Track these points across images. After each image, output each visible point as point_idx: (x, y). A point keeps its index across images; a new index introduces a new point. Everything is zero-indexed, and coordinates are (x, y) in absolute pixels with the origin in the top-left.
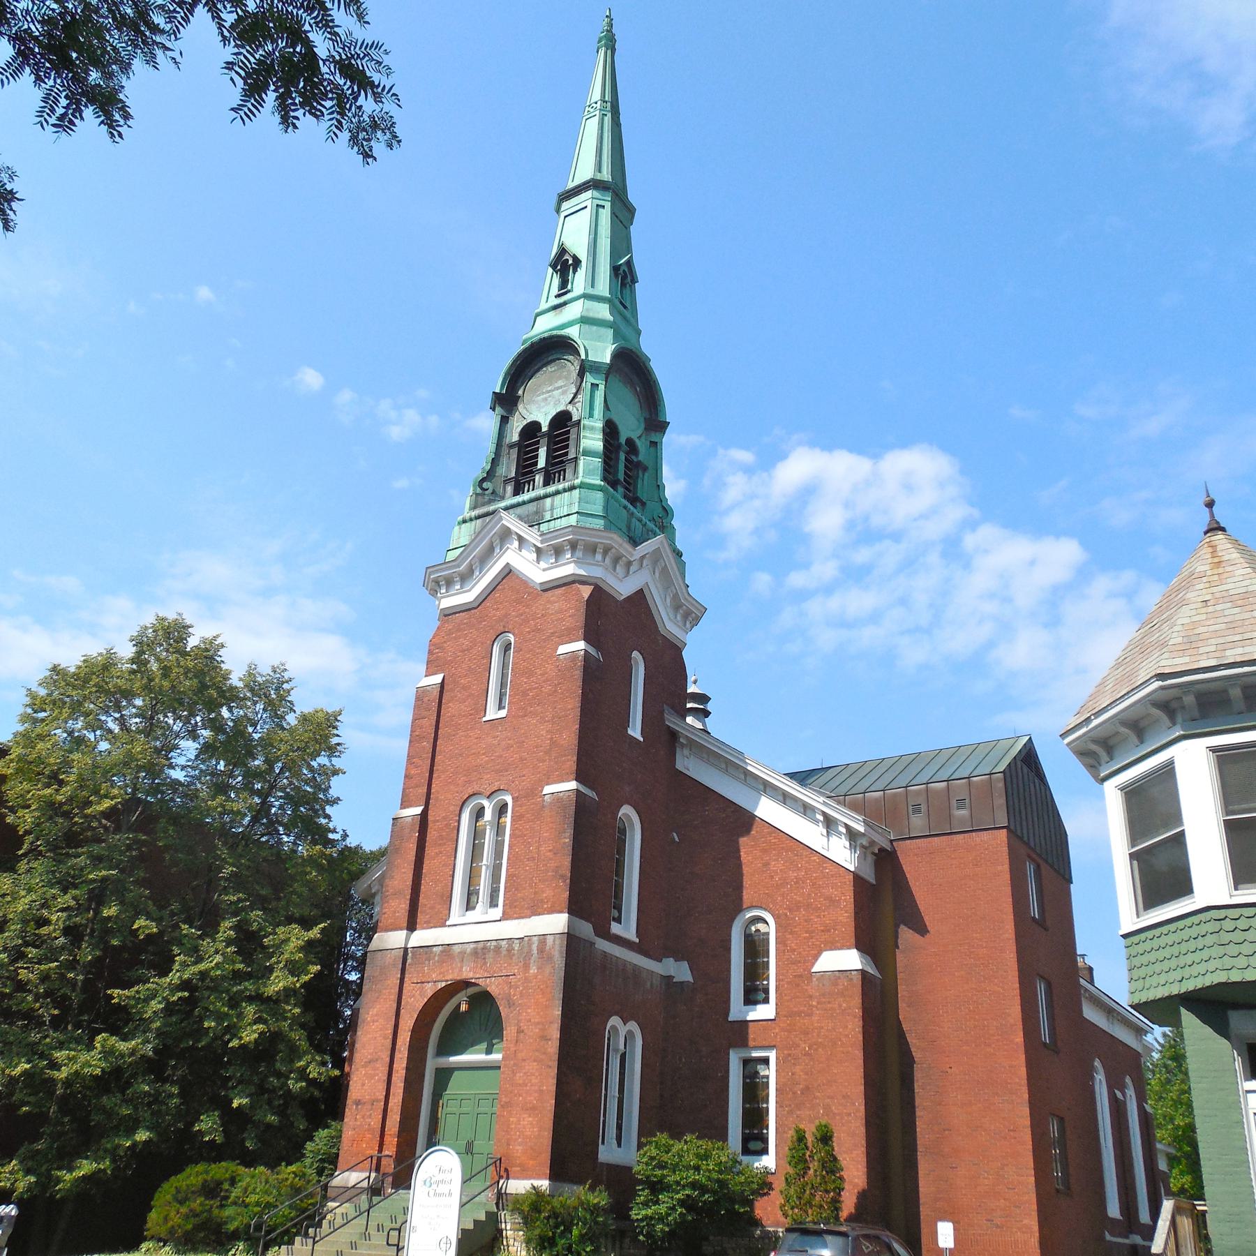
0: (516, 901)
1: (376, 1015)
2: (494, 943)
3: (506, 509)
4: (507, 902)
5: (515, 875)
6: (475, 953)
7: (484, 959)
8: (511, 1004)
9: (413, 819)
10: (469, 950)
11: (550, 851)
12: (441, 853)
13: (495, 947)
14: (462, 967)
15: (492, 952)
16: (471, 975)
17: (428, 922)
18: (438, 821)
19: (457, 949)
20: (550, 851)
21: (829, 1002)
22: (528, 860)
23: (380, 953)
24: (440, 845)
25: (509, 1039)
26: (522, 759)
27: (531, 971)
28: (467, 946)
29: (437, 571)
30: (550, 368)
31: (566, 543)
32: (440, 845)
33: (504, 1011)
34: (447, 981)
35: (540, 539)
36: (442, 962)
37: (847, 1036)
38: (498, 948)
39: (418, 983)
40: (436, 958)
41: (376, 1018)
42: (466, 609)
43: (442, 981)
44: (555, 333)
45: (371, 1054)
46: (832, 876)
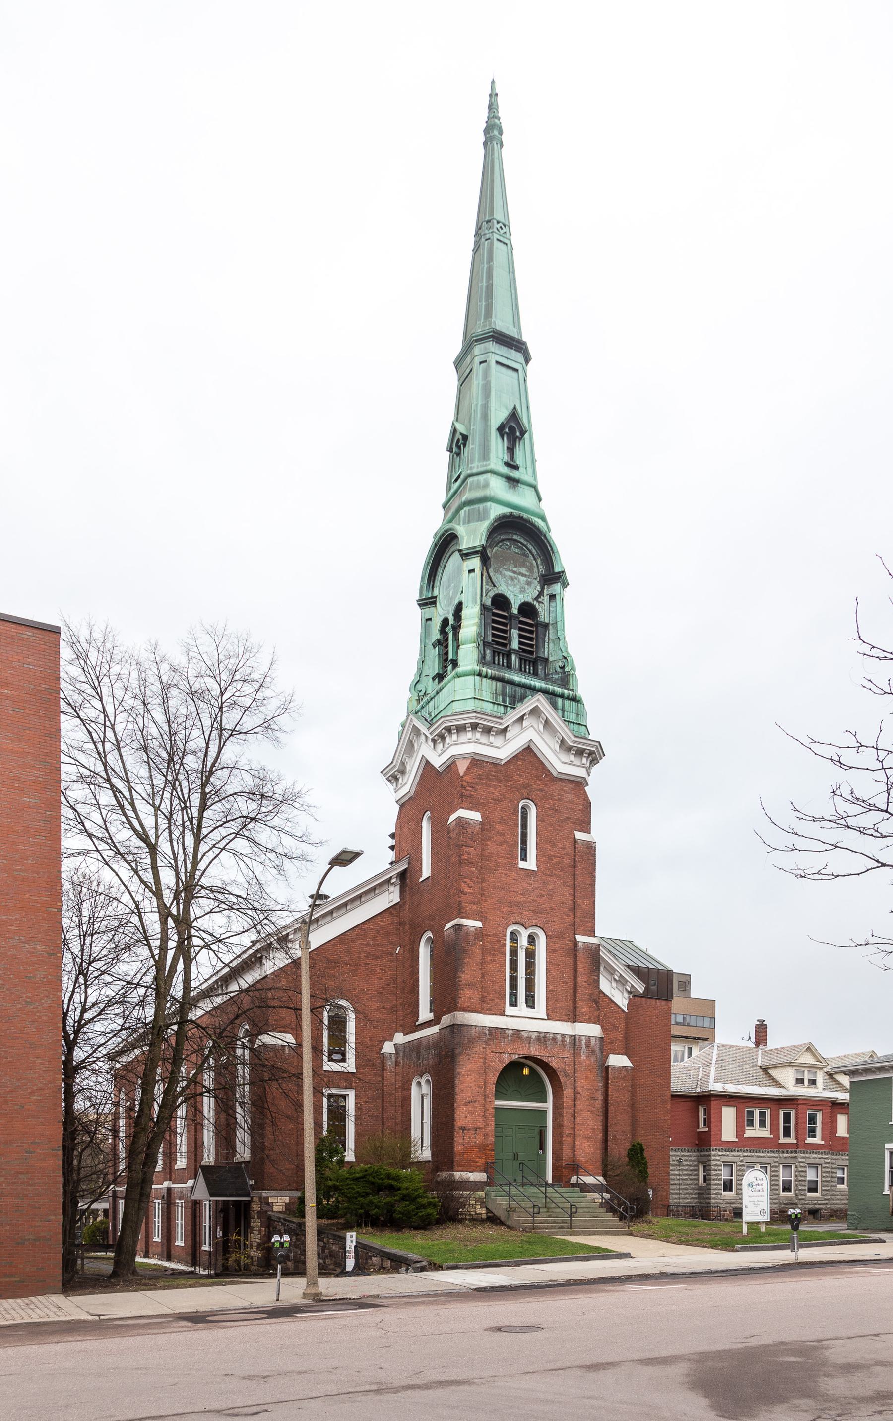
0: (556, 1009)
1: (469, 1071)
2: (552, 1035)
5: (554, 991)
6: (538, 1039)
7: (546, 1044)
10: (534, 1037)
14: (529, 1047)
16: (537, 1053)
19: (525, 1035)
28: (532, 1033)
34: (519, 1054)
45: (470, 1097)
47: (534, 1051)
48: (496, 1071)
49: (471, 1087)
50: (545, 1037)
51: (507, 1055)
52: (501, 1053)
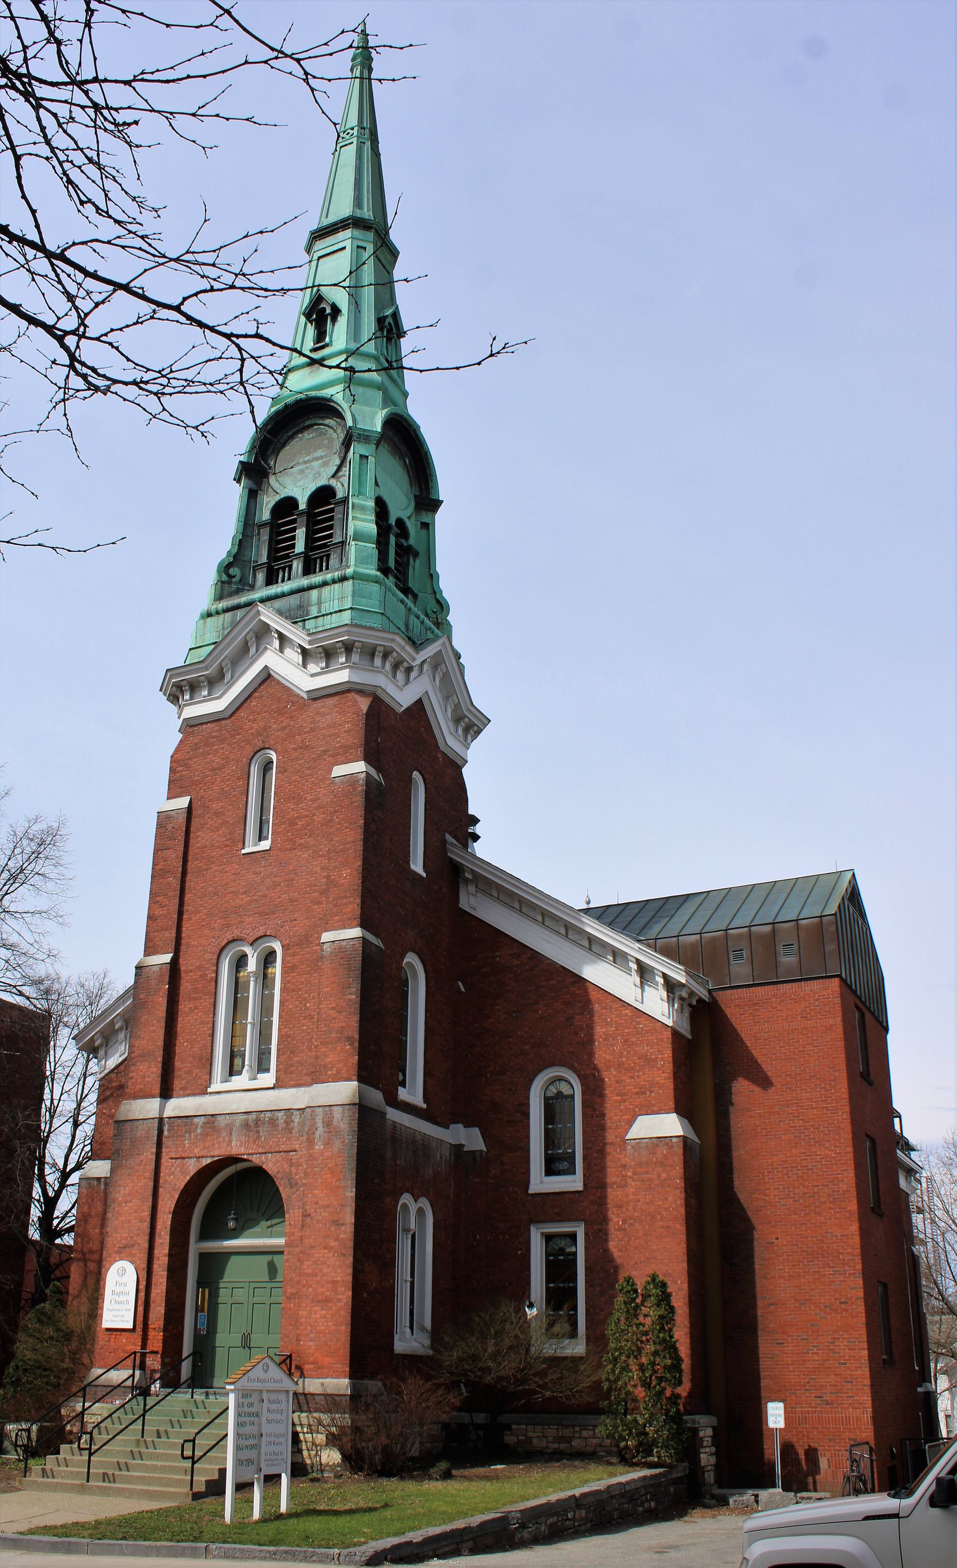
0: (292, 1065)
1: (129, 1195)
2: (268, 1114)
3: (263, 601)
4: (281, 1067)
5: (289, 1036)
7: (258, 1132)
8: (292, 1184)
9: (161, 969)
10: (238, 1123)
11: (333, 1008)
12: (196, 1008)
13: (271, 1119)
15: (266, 1125)
16: (243, 1150)
17: (184, 1089)
18: (191, 971)
19: (222, 1122)
20: (333, 1008)
21: (647, 1173)
22: (305, 1018)
23: (130, 1124)
24: (195, 999)
25: (292, 1223)
26: (292, 900)
27: (317, 1147)
28: (235, 1117)
29: (180, 674)
30: (308, 435)
31: (340, 644)
32: (195, 999)
33: (284, 1192)
34: (214, 1156)
35: (308, 638)
36: (205, 1135)
37: (667, 1209)
38: (273, 1122)
39: (176, 1158)
40: (199, 1131)
41: (128, 1198)
42: (215, 719)
43: (207, 1157)
44: (313, 394)
45: (126, 1238)
46: (647, 1032)
47: (236, 1147)
48: (174, 1190)
49: (129, 1221)
50: (257, 1121)
51: (193, 1160)
52: (184, 1158)
